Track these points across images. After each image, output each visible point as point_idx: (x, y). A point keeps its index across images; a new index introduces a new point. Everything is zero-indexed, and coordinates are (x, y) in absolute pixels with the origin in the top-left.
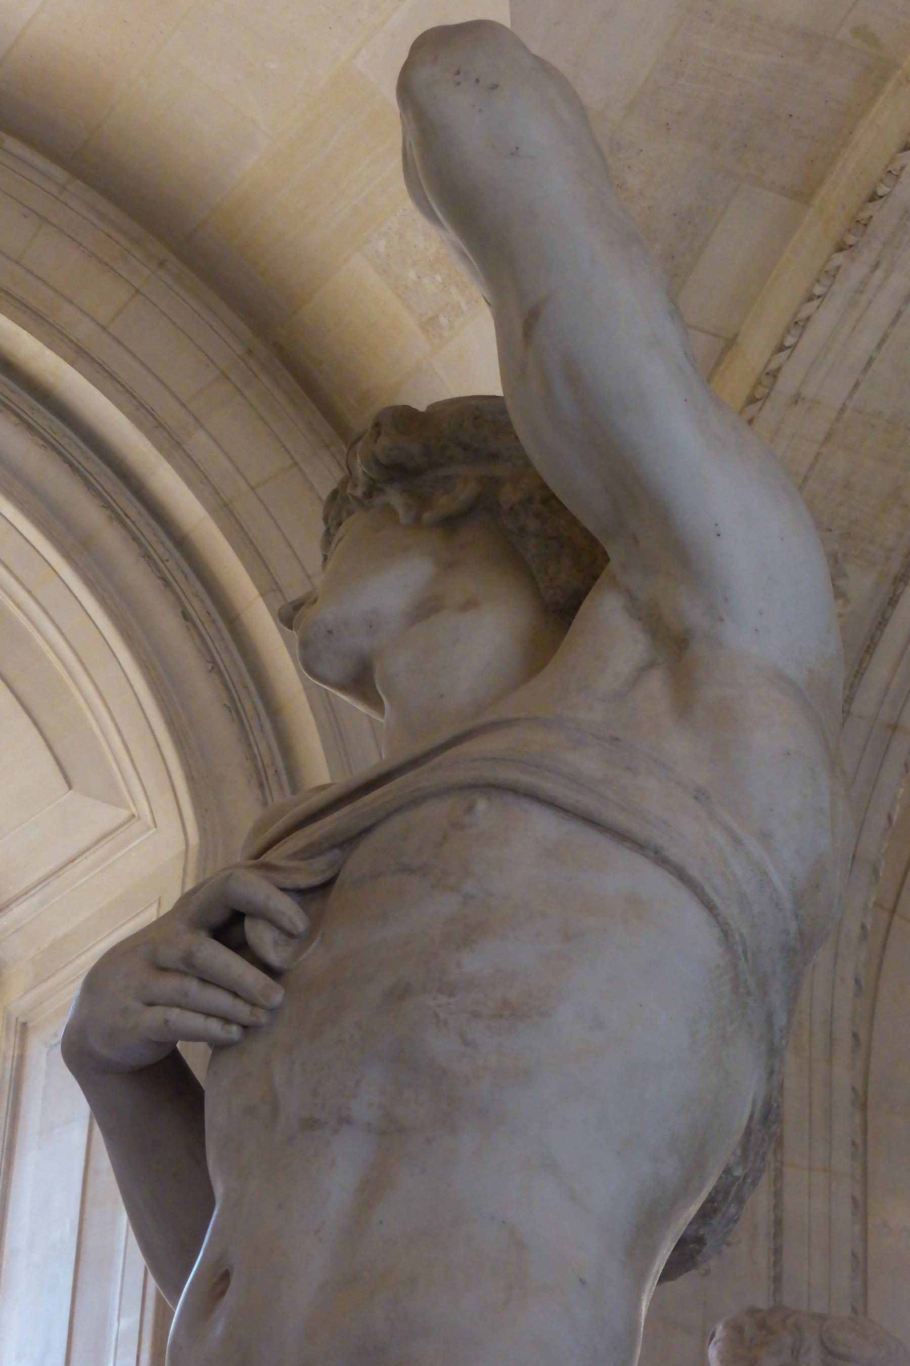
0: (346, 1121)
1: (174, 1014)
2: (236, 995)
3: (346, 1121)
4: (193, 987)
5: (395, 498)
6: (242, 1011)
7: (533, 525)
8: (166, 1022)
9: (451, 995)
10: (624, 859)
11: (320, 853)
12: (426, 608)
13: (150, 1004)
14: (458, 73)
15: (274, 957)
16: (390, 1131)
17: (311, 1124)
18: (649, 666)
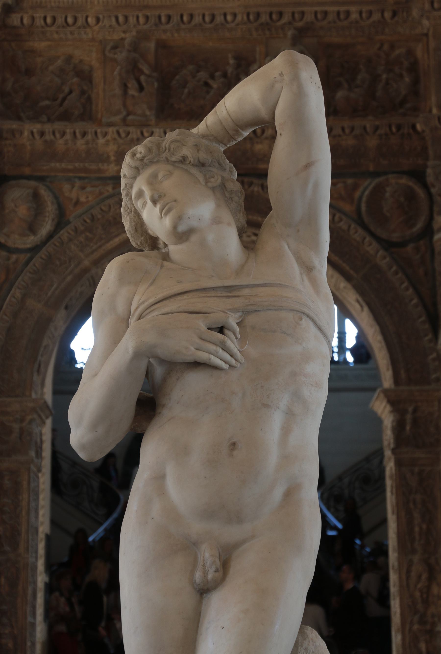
0: (278, 408)
1: (212, 357)
2: (231, 356)
3: (278, 408)
4: (221, 351)
5: (195, 171)
6: (233, 362)
7: (236, 199)
8: (210, 359)
9: (306, 378)
10: (325, 342)
11: (237, 312)
12: (216, 221)
13: (196, 349)
14: (311, 78)
15: (237, 346)
16: (290, 414)
17: (267, 406)
18: (301, 274)
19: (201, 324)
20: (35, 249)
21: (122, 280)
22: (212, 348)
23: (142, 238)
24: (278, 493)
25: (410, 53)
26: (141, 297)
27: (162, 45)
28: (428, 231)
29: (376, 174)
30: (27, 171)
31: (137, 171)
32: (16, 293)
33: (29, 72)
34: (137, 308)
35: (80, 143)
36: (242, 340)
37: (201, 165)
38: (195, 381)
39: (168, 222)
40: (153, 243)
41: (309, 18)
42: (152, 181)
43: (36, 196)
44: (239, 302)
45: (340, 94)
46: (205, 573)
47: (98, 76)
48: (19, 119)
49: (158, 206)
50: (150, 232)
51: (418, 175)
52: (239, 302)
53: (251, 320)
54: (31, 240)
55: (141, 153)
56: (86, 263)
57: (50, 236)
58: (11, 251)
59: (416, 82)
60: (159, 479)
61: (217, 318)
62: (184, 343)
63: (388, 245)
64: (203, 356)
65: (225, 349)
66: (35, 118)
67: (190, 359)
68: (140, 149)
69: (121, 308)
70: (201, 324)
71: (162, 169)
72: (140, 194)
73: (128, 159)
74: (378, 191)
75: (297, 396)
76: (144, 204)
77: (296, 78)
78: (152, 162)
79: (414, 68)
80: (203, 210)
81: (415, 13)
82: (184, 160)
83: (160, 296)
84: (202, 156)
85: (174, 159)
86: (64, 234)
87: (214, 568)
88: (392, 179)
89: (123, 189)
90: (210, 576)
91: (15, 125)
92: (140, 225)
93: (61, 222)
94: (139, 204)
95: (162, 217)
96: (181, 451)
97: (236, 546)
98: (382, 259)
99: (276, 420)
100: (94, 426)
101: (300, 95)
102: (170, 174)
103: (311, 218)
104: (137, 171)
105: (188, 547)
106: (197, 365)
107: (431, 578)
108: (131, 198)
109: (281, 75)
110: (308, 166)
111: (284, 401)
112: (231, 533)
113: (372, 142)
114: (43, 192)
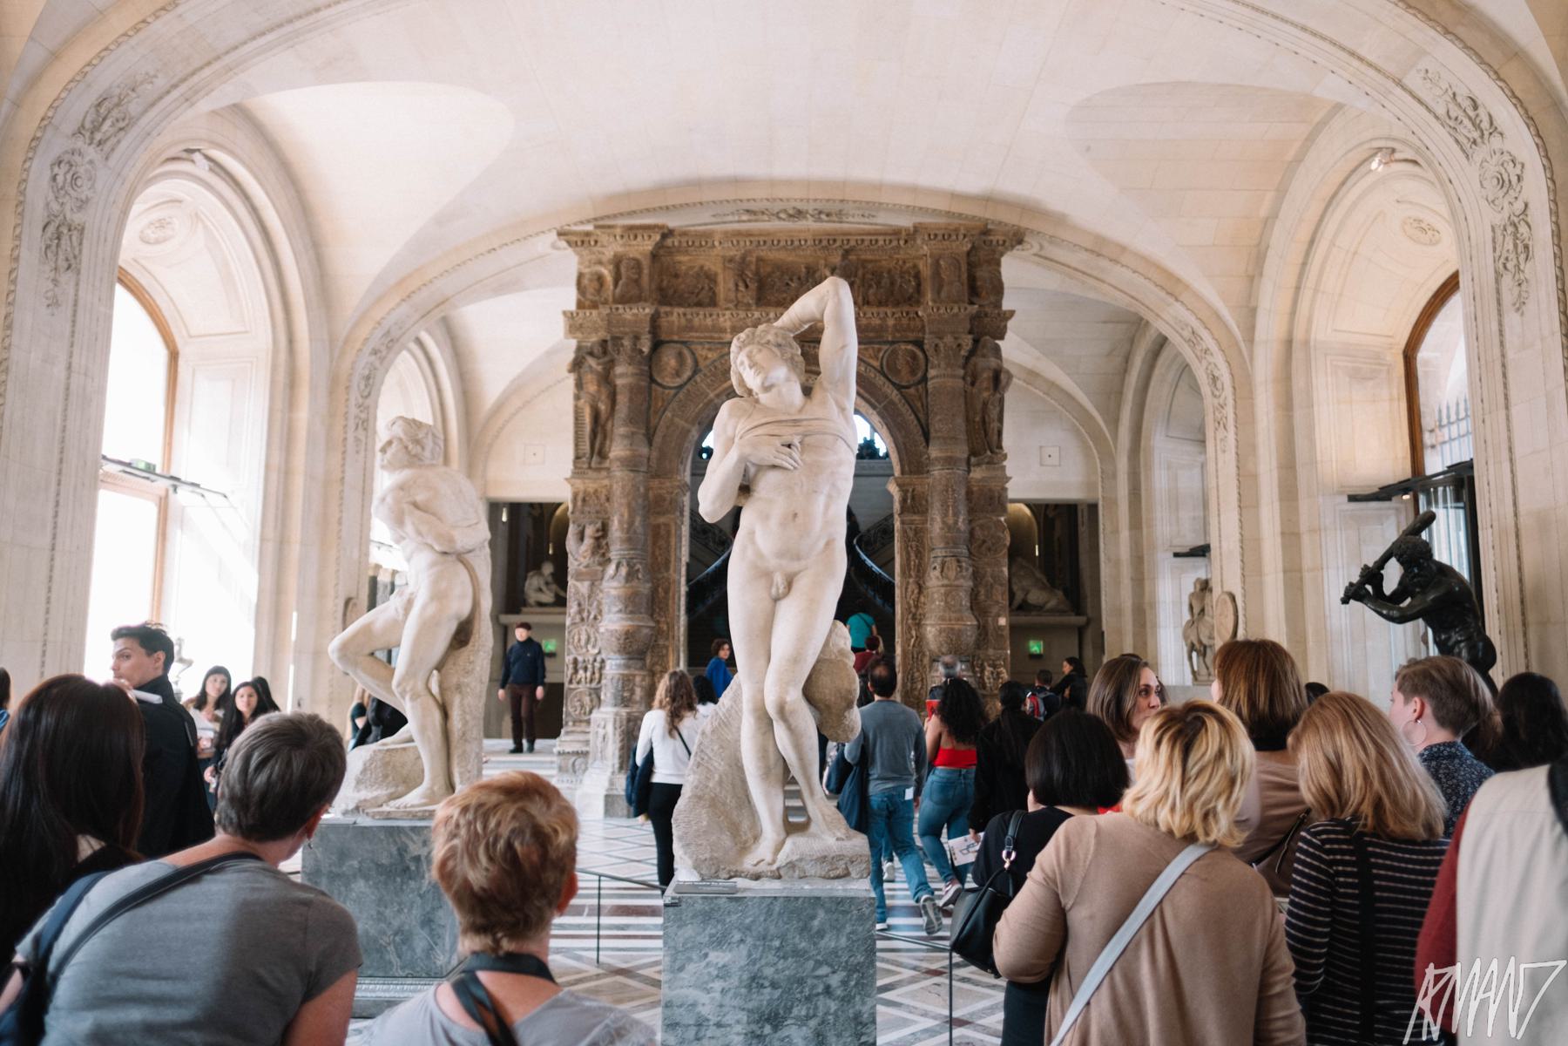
12: (788, 380)
16: (830, 497)
19: (777, 442)
20: (681, 387)
21: (731, 415)
24: (822, 544)
25: (915, 266)
26: (743, 426)
27: (759, 259)
28: (925, 379)
29: (893, 343)
30: (676, 338)
31: (740, 349)
32: (668, 414)
33: (677, 276)
35: (709, 321)
36: (802, 453)
37: (779, 346)
40: (750, 392)
41: (853, 243)
43: (680, 355)
44: (800, 430)
45: (871, 291)
47: (720, 278)
48: (670, 305)
51: (919, 344)
52: (800, 430)
53: (807, 440)
54: (678, 381)
56: (712, 395)
57: (690, 379)
58: (664, 387)
59: (919, 285)
60: (752, 533)
61: (787, 439)
63: (899, 387)
64: (778, 462)
66: (680, 305)
68: (742, 335)
69: (730, 433)
70: (777, 442)
71: (754, 348)
73: (735, 341)
74: (894, 352)
75: (834, 485)
77: (837, 294)
79: (917, 276)
80: (781, 372)
81: (919, 242)
84: (780, 340)
86: (698, 378)
88: (903, 347)
91: (668, 309)
92: (742, 382)
93: (696, 371)
94: (741, 369)
96: (765, 518)
97: (796, 574)
98: (894, 395)
99: (821, 500)
100: (713, 503)
101: (839, 304)
103: (845, 380)
104: (740, 349)
105: (767, 575)
106: (774, 467)
107: (920, 592)
110: (844, 347)
111: (826, 489)
112: (794, 566)
113: (891, 322)
114: (686, 352)
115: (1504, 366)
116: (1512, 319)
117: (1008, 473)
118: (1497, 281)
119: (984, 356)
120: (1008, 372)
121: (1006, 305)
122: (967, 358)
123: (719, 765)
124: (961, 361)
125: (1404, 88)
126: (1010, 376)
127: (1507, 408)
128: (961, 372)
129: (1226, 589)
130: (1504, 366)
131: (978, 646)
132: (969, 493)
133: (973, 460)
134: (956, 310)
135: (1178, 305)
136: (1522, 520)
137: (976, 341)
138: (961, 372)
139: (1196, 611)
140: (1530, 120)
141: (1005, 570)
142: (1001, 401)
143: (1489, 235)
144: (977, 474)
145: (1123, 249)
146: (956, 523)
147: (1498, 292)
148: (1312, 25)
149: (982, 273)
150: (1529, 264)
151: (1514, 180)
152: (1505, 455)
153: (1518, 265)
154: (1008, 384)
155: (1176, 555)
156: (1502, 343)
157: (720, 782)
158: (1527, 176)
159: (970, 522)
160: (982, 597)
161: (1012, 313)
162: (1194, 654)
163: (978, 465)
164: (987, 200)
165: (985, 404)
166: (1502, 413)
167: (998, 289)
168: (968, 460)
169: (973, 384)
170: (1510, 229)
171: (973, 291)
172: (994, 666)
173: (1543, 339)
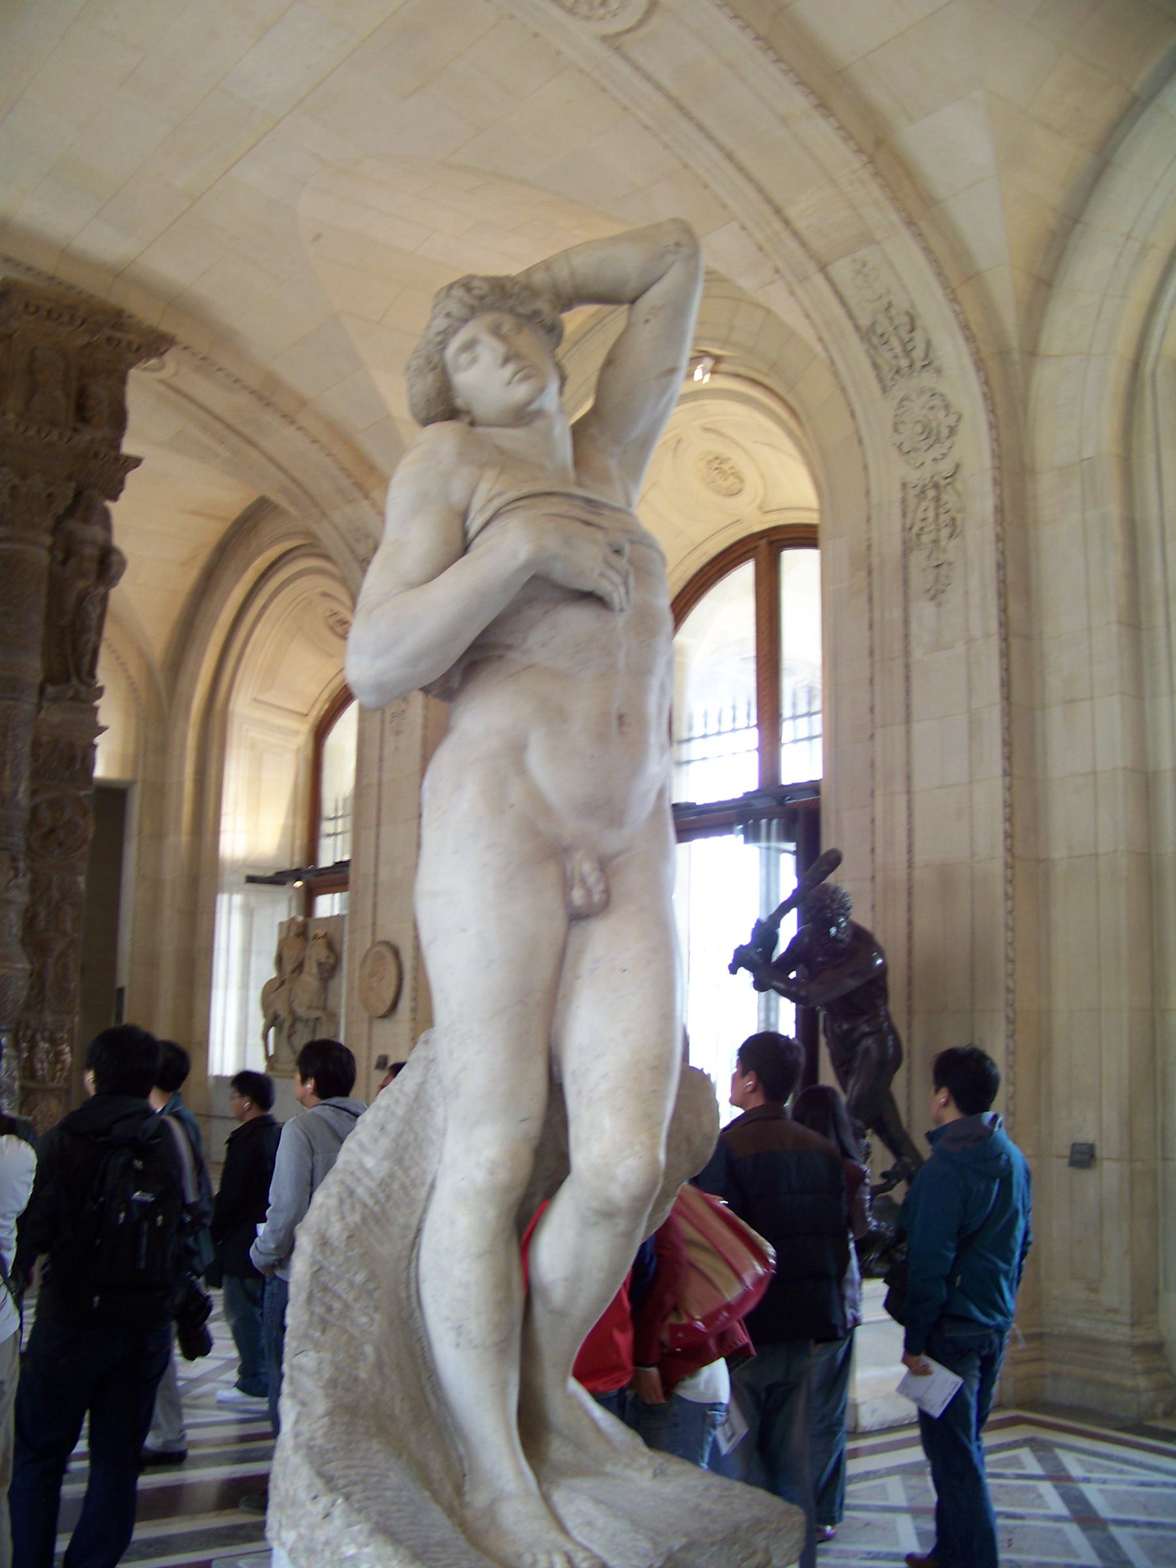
22: (617, 579)
23: (442, 408)
31: (473, 312)
34: (490, 501)
38: (577, 621)
39: (521, 392)
42: (496, 331)
46: (589, 892)
49: (510, 369)
50: (459, 402)
55: (480, 288)
62: (587, 563)
65: (626, 583)
67: (587, 586)
69: (458, 493)
72: (470, 345)
76: (474, 361)
78: (492, 308)
82: (536, 313)
83: (526, 489)
85: (521, 310)
87: (601, 887)
89: (438, 334)
90: (597, 897)
95: (509, 383)
96: (555, 716)
102: (519, 329)
108: (444, 349)
109: (677, 244)
115: (907, 666)
116: (924, 610)
117: (103, 719)
118: (905, 554)
119: (86, 521)
120: (118, 552)
121: (129, 447)
122: (60, 520)
123: (369, 1323)
124: (49, 522)
125: (829, 279)
126: (123, 564)
127: (908, 720)
128: (48, 540)
129: (381, 937)
130: (907, 666)
131: (28, 1007)
132: (36, 744)
133: (50, 689)
134: (54, 436)
135: (365, 504)
136: (917, 874)
137: (78, 494)
138: (48, 540)
139: (288, 967)
140: (979, 364)
141: (81, 880)
142: (104, 599)
143: (897, 495)
144: (53, 715)
145: (303, 403)
146: (15, 793)
147: (905, 568)
148: (743, 155)
149: (99, 391)
150: (953, 543)
151: (945, 432)
152: (899, 785)
153: (936, 542)
154: (119, 575)
155: (251, 880)
156: (906, 636)
157: (379, 1365)
158: (964, 431)
159: (34, 793)
160: (41, 924)
161: (136, 462)
162: (272, 1030)
163: (56, 699)
164: (118, 273)
165: (81, 599)
166: (899, 731)
167: (119, 419)
168: (42, 691)
169: (64, 562)
170: (931, 493)
171: (82, 411)
172: (53, 1041)
173: (969, 641)
